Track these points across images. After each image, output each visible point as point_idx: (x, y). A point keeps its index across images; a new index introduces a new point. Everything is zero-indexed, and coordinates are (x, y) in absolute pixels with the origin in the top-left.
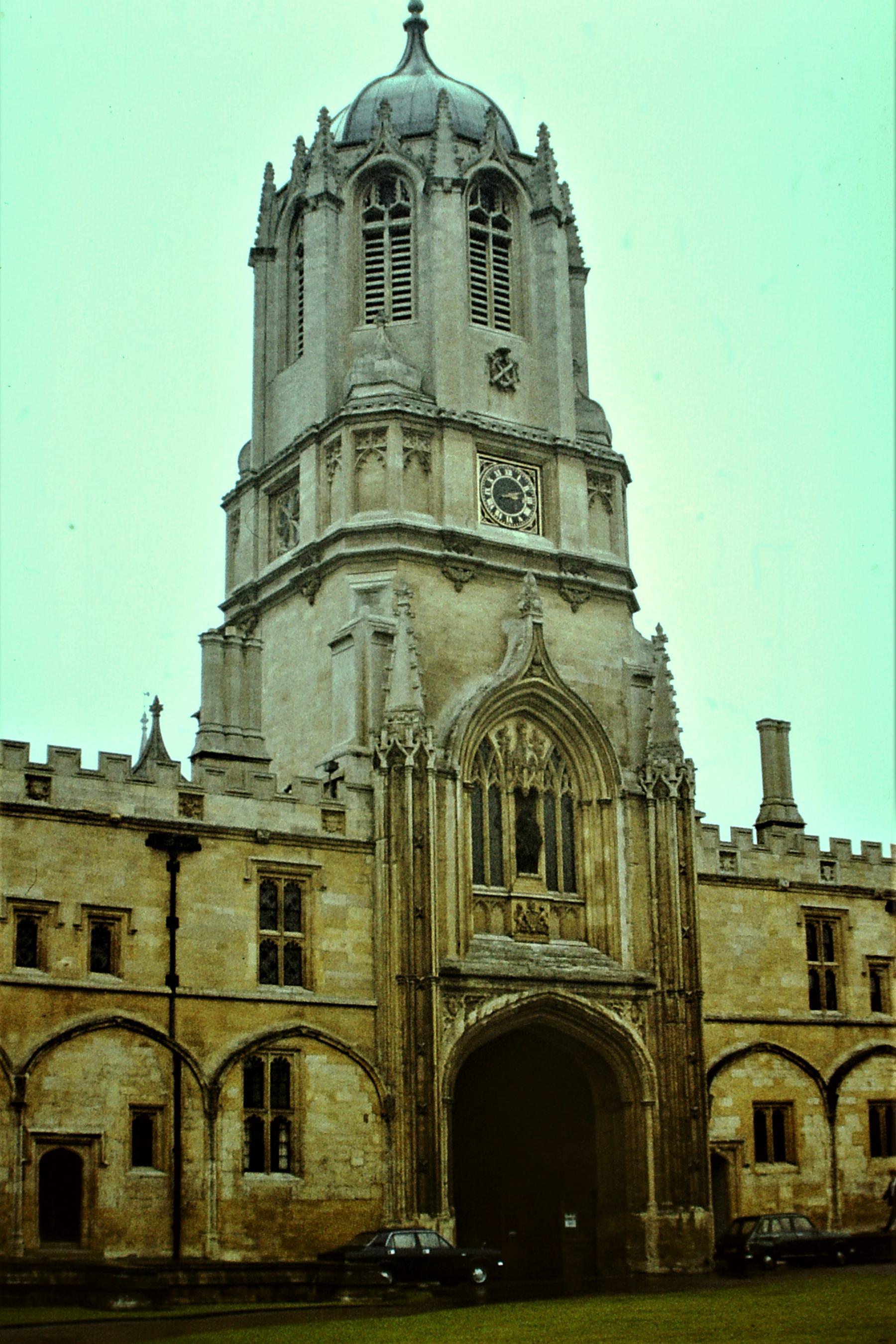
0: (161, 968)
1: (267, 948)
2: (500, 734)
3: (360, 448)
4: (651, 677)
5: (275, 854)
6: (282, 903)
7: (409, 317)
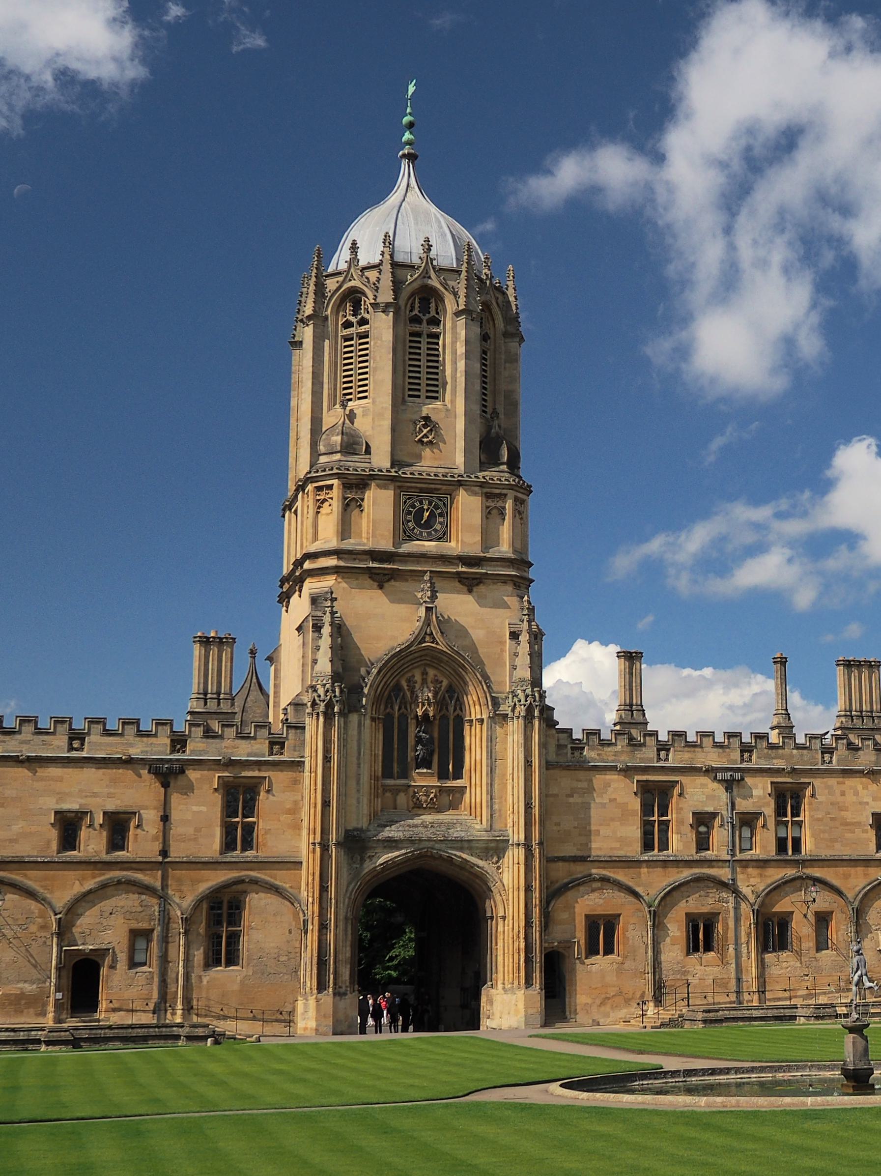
0: (157, 846)
2: (408, 681)
3: (318, 498)
7: (366, 397)
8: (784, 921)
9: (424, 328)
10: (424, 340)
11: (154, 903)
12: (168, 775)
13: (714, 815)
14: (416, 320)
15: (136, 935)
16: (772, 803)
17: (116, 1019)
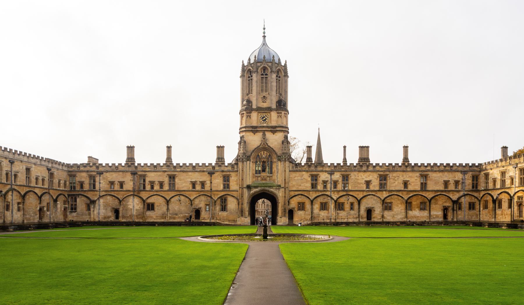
0: (210, 188)
1: (224, 185)
4: (286, 142)
5: (224, 173)
6: (226, 179)
8: (343, 204)
9: (264, 76)
10: (264, 79)
11: (209, 198)
12: (211, 174)
13: (327, 181)
14: (262, 75)
15: (207, 205)
16: (341, 178)
17: (203, 221)
